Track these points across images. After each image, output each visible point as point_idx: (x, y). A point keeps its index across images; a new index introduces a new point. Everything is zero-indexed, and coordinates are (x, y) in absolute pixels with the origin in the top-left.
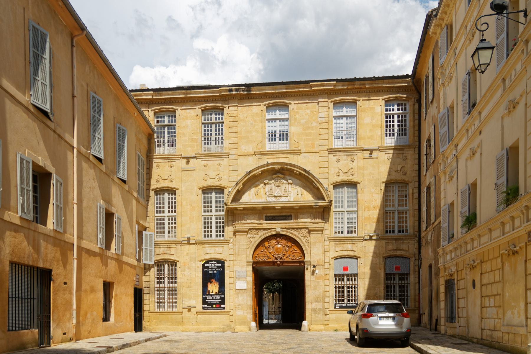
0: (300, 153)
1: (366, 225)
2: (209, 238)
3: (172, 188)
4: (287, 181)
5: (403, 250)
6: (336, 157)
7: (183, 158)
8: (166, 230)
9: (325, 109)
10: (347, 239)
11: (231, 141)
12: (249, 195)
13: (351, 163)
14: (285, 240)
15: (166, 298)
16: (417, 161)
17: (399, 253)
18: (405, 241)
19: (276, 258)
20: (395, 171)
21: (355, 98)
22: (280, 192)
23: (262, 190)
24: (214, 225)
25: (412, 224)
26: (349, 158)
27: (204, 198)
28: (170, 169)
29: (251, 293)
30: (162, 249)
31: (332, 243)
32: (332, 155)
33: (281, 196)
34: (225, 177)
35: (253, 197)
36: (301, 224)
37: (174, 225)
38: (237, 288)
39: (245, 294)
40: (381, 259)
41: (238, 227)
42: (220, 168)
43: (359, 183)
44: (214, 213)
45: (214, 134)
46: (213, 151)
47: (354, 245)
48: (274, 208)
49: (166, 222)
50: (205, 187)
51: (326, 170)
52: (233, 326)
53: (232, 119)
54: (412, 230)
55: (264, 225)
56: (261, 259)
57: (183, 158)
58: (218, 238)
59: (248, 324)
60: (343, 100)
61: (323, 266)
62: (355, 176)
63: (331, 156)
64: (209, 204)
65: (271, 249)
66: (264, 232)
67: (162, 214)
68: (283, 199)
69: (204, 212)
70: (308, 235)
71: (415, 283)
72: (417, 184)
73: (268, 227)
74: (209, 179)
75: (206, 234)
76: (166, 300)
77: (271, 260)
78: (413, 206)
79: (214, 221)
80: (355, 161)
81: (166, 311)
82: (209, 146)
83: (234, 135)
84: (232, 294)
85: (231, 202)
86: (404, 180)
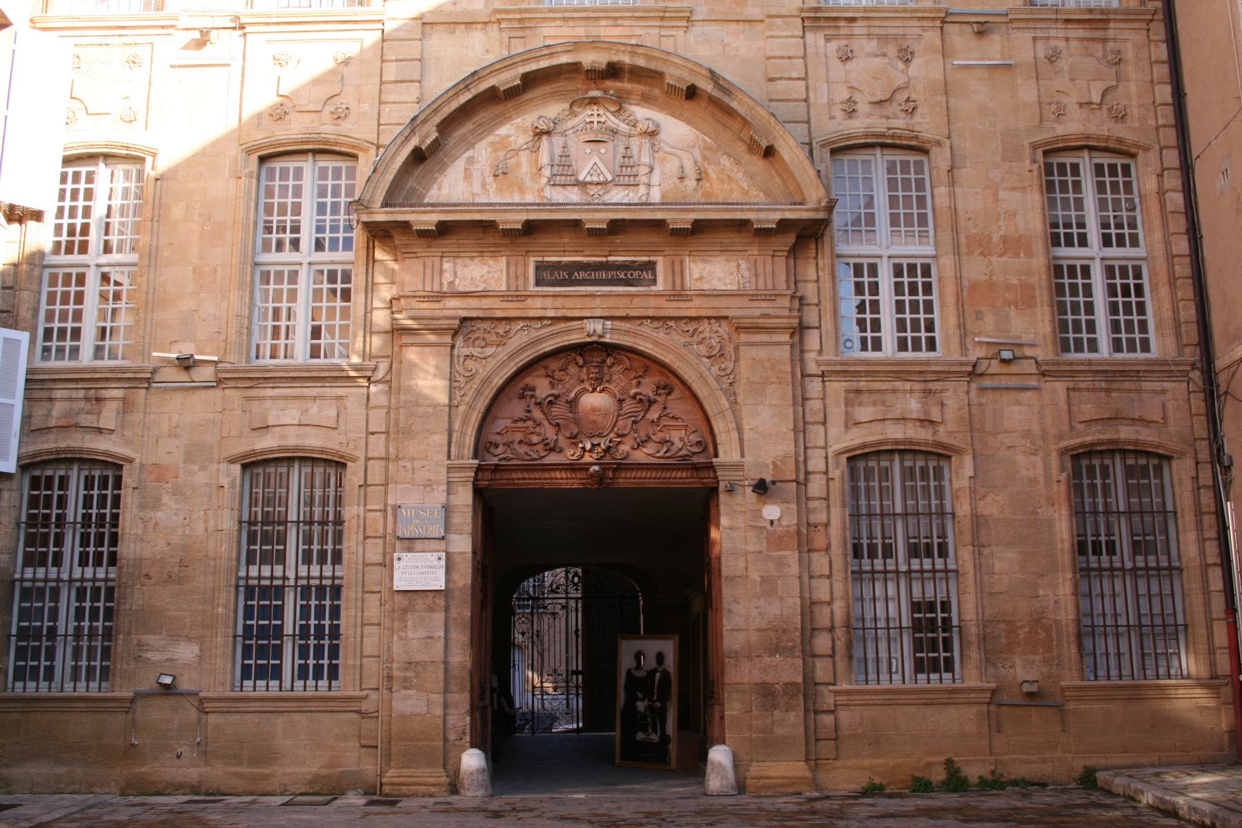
1: (979, 315)
5: (1146, 422)
6: (833, 45)
10: (899, 372)
12: (468, 176)
13: (901, 65)
16: (1163, 71)
17: (1126, 433)
18: (1146, 385)
20: (1081, 105)
25: (1167, 313)
31: (837, 387)
34: (365, 107)
35: (484, 185)
36: (697, 302)
38: (400, 584)
40: (1054, 460)
43: (939, 143)
54: (1170, 341)
61: (802, 483)
62: (917, 118)
63: (815, 39)
67: (76, 258)
68: (617, 195)
71: (1205, 567)
72: (1172, 158)
73: (551, 313)
78: (1167, 244)
80: (916, 63)
81: (55, 693)
84: (373, 610)
85: (386, 204)
86: (1119, 140)
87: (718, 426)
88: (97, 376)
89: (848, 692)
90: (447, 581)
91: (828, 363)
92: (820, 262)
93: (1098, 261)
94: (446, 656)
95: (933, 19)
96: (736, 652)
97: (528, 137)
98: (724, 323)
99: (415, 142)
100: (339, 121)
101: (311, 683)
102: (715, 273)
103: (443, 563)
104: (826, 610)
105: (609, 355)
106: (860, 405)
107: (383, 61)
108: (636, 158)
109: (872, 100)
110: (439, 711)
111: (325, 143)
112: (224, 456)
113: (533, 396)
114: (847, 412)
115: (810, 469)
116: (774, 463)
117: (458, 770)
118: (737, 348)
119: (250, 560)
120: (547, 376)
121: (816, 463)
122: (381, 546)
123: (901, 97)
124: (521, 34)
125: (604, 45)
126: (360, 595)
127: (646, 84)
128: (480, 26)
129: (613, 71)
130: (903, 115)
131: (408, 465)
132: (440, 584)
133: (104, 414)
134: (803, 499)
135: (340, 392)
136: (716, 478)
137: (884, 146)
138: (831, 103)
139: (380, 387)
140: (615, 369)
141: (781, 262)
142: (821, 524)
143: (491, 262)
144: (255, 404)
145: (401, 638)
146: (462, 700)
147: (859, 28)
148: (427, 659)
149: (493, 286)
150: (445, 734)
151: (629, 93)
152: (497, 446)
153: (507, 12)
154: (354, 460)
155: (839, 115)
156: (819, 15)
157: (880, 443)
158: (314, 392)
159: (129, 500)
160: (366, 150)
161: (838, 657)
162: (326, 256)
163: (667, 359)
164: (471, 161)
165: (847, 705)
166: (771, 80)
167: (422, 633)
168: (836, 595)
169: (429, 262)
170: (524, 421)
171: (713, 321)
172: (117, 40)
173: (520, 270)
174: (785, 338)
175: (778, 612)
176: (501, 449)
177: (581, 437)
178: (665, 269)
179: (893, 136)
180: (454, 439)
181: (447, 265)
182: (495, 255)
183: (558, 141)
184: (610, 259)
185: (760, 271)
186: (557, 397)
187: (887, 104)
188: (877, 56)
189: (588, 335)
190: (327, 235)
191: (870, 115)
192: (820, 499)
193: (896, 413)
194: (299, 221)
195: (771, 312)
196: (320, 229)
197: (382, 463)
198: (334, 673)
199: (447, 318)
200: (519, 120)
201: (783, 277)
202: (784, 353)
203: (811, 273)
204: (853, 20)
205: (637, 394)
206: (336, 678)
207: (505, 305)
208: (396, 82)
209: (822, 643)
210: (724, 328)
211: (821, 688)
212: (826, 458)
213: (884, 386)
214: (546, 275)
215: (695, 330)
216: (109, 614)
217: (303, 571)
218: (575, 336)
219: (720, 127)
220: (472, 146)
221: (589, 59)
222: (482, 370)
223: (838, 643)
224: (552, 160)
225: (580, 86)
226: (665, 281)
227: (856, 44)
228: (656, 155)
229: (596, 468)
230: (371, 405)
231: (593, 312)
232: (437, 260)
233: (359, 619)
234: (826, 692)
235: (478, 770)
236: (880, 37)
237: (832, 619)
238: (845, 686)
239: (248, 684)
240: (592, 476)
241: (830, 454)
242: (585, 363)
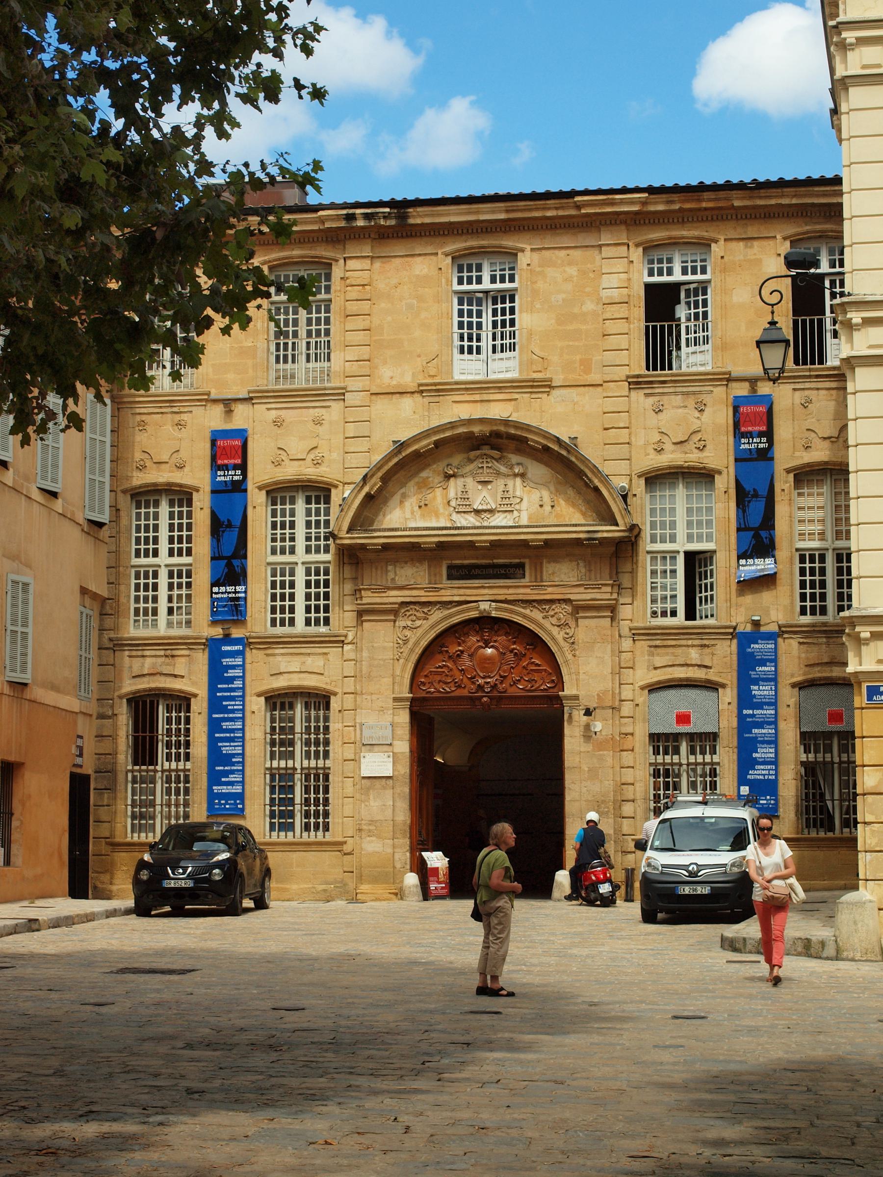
0: (550, 386)
2: (287, 630)
3: (181, 485)
4: (511, 467)
6: (651, 400)
7: (215, 401)
8: (163, 605)
9: (621, 265)
11: (352, 354)
13: (697, 414)
14: (507, 634)
15: (158, 801)
19: (480, 688)
21: (705, 234)
22: (489, 500)
23: (439, 492)
24: (300, 591)
26: (691, 402)
27: (274, 515)
28: (176, 434)
29: (407, 790)
30: (148, 661)
31: (643, 645)
32: (641, 393)
33: (491, 511)
35: (412, 513)
36: (550, 590)
37: (184, 592)
38: (365, 773)
39: (389, 792)
41: (369, 598)
42: (320, 430)
44: (301, 555)
45: (303, 333)
46: (300, 383)
47: (707, 650)
48: (471, 545)
49: (163, 580)
50: (275, 483)
51: (624, 435)
52: (351, 886)
53: (353, 293)
55: (443, 592)
56: (434, 689)
57: (215, 401)
58: (312, 629)
60: (670, 238)
62: (706, 453)
63: (638, 396)
64: (287, 531)
65: (466, 661)
66: (447, 612)
67: (151, 560)
68: (499, 520)
69: (274, 552)
70: (572, 624)
73: (456, 599)
74: (287, 462)
75: (278, 616)
76: (158, 808)
77: (465, 692)
79: (300, 578)
80: (708, 410)
82: (289, 365)
83: (360, 337)
84: (349, 790)
87: (564, 670)
88: (172, 641)
93: (830, 551)
99: (366, 489)
101: (312, 833)
103: (391, 759)
108: (511, 492)
112: (253, 692)
113: (447, 651)
116: (598, 695)
119: (272, 758)
123: (696, 438)
124: (436, 399)
129: (497, 435)
130: (697, 451)
131: (369, 697)
133: (177, 665)
135: (325, 650)
139: (350, 646)
144: (271, 659)
153: (427, 385)
154: (335, 694)
158: (308, 651)
159: (196, 720)
160: (336, 487)
164: (404, 496)
166: (606, 429)
172: (169, 410)
179: (688, 468)
183: (460, 482)
186: (462, 652)
187: (686, 444)
188: (681, 407)
194: (294, 533)
195: (598, 596)
198: (326, 828)
199: (391, 604)
200: (435, 466)
206: (328, 830)
214: (454, 572)
216: (187, 791)
217: (306, 763)
231: (485, 597)
239: (274, 834)
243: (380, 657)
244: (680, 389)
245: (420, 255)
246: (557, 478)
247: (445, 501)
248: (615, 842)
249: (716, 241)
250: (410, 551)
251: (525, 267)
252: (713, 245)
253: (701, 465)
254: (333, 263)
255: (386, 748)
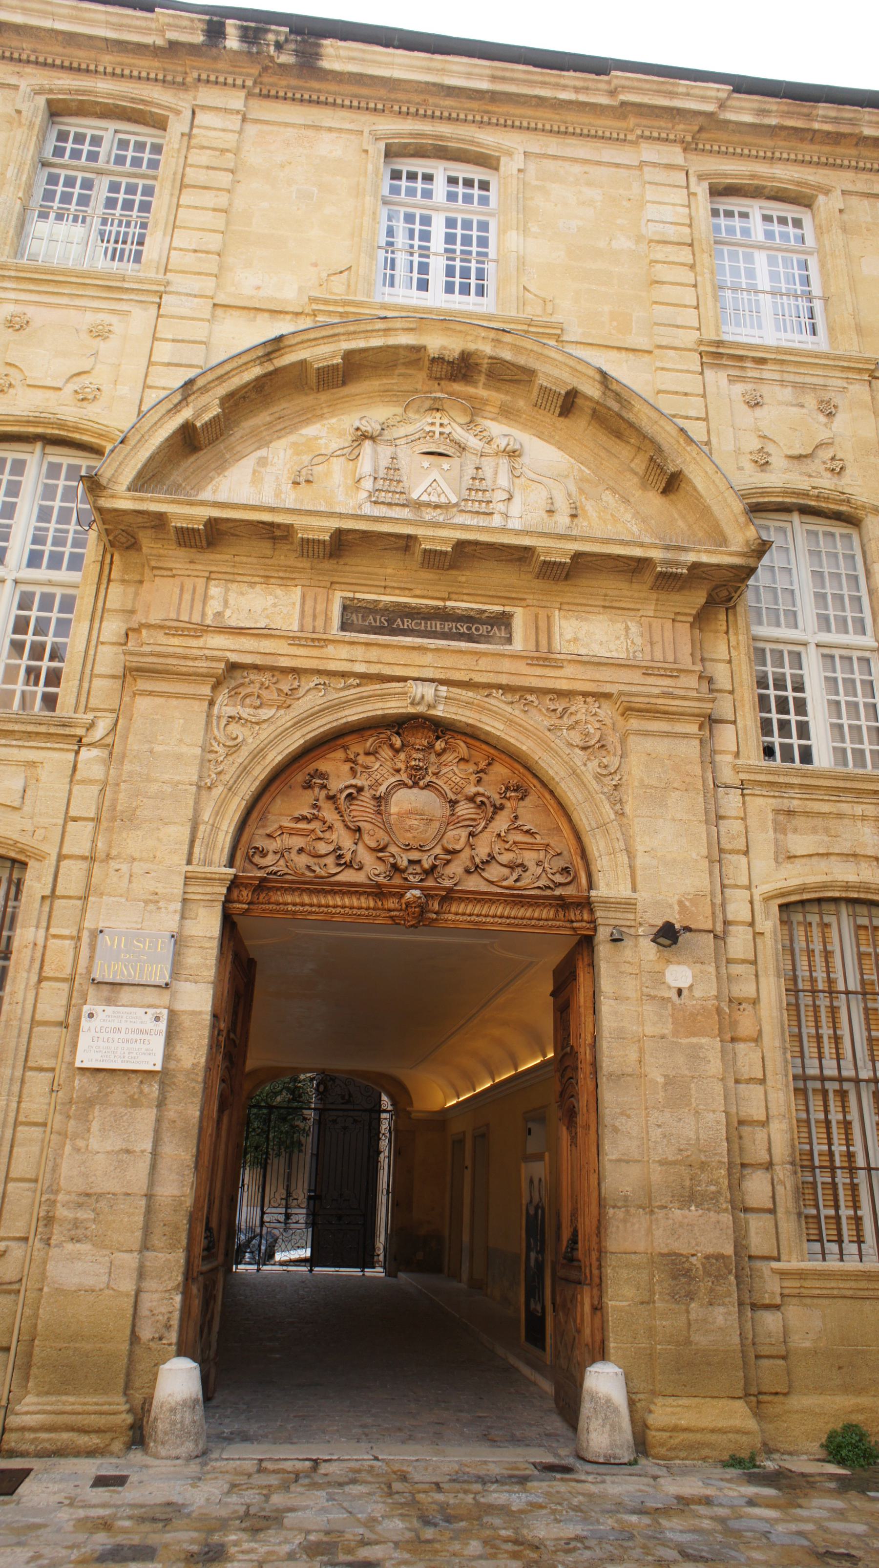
6: (739, 388)
12: (256, 478)
13: (822, 419)
29: (194, 1112)
31: (762, 805)
38: (86, 1058)
55: (331, 650)
59: (134, 1377)
61: (720, 938)
63: (717, 379)
73: (360, 668)
87: (597, 846)
89: (801, 1275)
90: (167, 1057)
91: (750, 770)
92: (732, 638)
94: (152, 1183)
95: (860, 371)
96: (626, 1198)
97: (346, 441)
98: (606, 704)
99: (186, 414)
100: (85, 403)
102: (596, 635)
103: (163, 1026)
104: (760, 1134)
105: (438, 738)
106: (795, 830)
107: (154, 338)
109: (790, 453)
110: (128, 1285)
111: (62, 425)
113: (324, 787)
114: (776, 840)
115: (730, 917)
116: (680, 903)
117: (148, 1400)
118: (623, 741)
120: (348, 760)
121: (738, 909)
122: (65, 994)
123: (825, 454)
125: (458, 327)
126: (18, 1073)
127: (507, 393)
128: (288, 317)
130: (828, 475)
131: (124, 867)
132: (153, 1061)
134: (723, 959)
136: (593, 921)
137: (805, 511)
138: (738, 452)
139: (95, 752)
140: (449, 757)
141: (684, 630)
142: (746, 999)
143: (279, 592)
145: (78, 1150)
146: (170, 1261)
147: (769, 372)
148: (117, 1190)
149: (278, 623)
150: (134, 1326)
151: (485, 402)
152: (264, 854)
153: (326, 302)
154: (41, 857)
155: (749, 467)
156: (721, 350)
157: (825, 886)
161: (780, 1211)
162: (42, 573)
163: (525, 745)
164: (263, 462)
165: (799, 1296)
167: (114, 1143)
168: (773, 1111)
169: (189, 583)
170: (309, 821)
171: (590, 699)
173: (320, 607)
174: (693, 728)
175: (692, 1135)
176: (269, 860)
177: (393, 849)
178: (525, 624)
180: (200, 834)
181: (215, 590)
182: (285, 582)
183: (385, 452)
184: (448, 603)
185: (657, 637)
186: (360, 790)
187: (809, 461)
189: (412, 703)
190: (48, 548)
191: (787, 470)
192: (744, 961)
193: (844, 846)
196: (38, 539)
197: (84, 865)
199: (207, 658)
200: (333, 421)
201: (688, 649)
202: (691, 749)
203: (721, 650)
204: (762, 361)
205: (478, 794)
207: (294, 650)
208: (169, 364)
209: (757, 1188)
210: (606, 711)
211: (758, 1264)
212: (751, 902)
213: (825, 808)
214: (357, 619)
215: (565, 710)
218: (393, 704)
219: (603, 454)
220: (267, 444)
221: (436, 343)
222: (251, 738)
223: (780, 1189)
224: (376, 471)
225: (419, 387)
226: (526, 640)
227: (765, 390)
228: (517, 481)
229: (417, 893)
230: (78, 776)
231: (420, 675)
232: (201, 582)
233: (12, 1115)
234: (767, 1272)
235: (184, 1403)
236: (795, 385)
237: (769, 1150)
238: (794, 1264)
240: (408, 904)
241: (757, 898)
242: (403, 745)
243: (166, 777)
244: (791, 378)
245: (330, 129)
246: (580, 470)
247: (350, 482)
248: (737, 1277)
249: (827, 192)
250: (266, 539)
251: (515, 172)
252: (821, 199)
253: (843, 497)
254: (172, 116)
255: (151, 996)
